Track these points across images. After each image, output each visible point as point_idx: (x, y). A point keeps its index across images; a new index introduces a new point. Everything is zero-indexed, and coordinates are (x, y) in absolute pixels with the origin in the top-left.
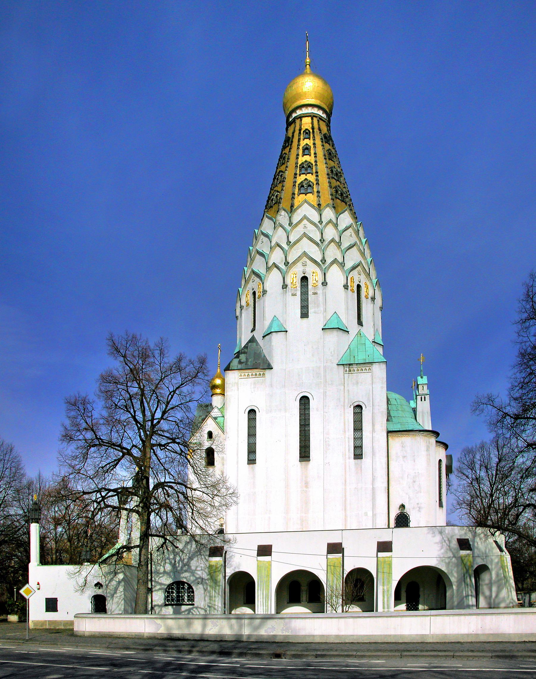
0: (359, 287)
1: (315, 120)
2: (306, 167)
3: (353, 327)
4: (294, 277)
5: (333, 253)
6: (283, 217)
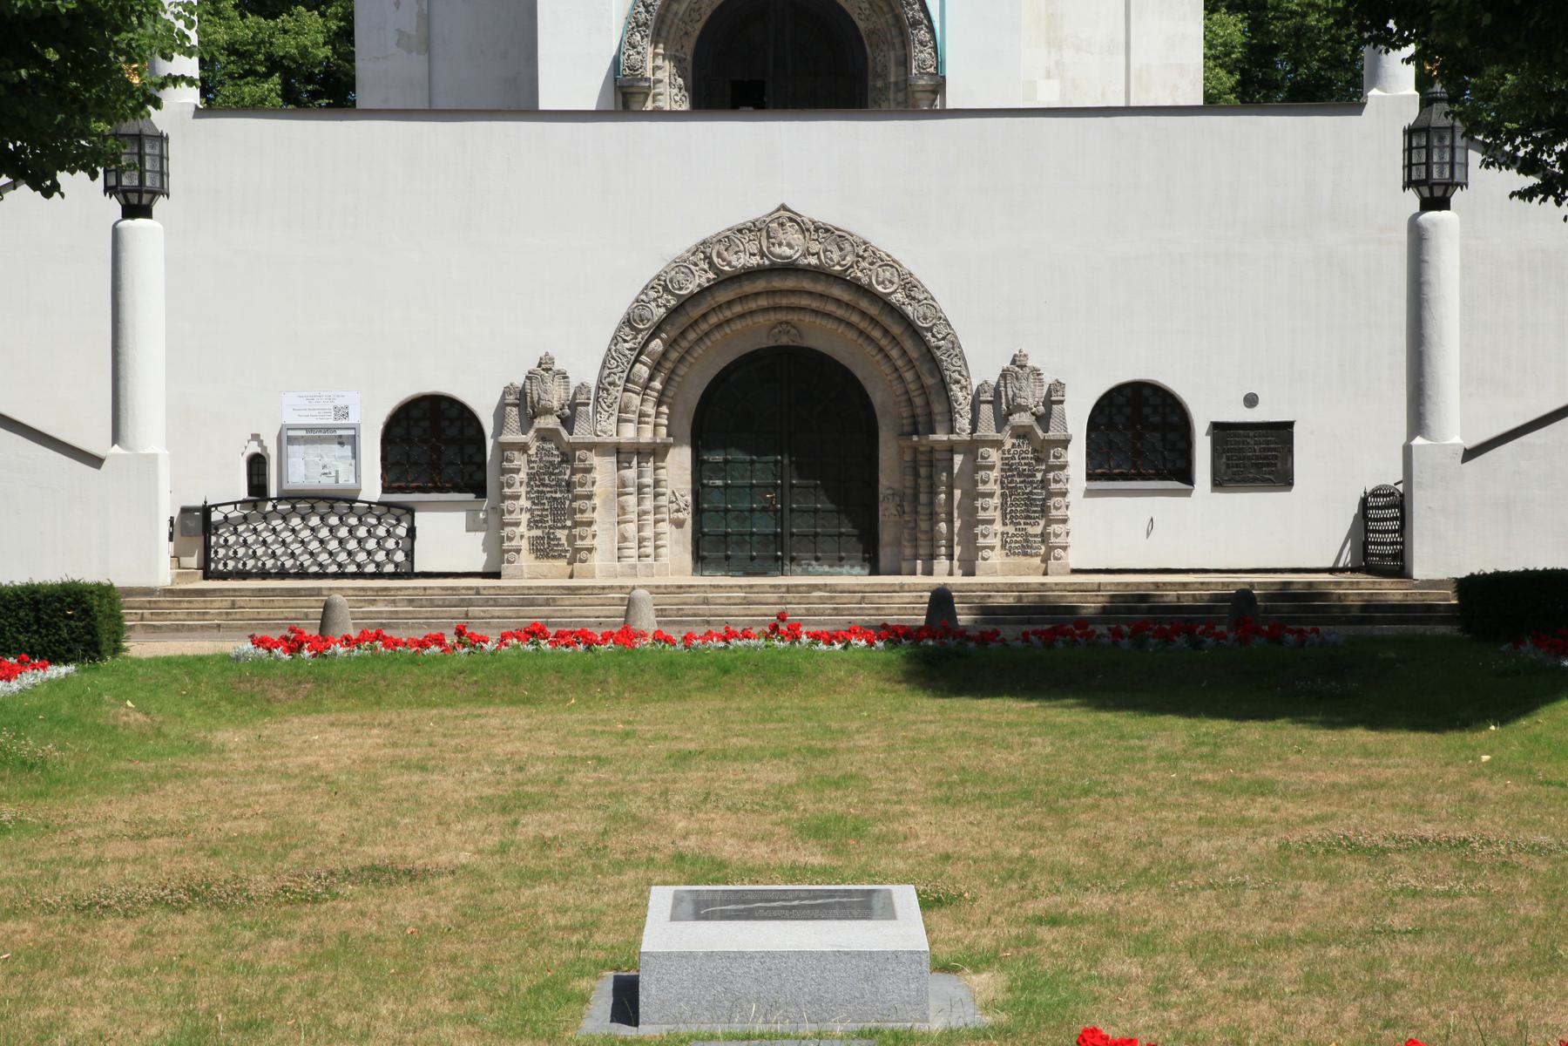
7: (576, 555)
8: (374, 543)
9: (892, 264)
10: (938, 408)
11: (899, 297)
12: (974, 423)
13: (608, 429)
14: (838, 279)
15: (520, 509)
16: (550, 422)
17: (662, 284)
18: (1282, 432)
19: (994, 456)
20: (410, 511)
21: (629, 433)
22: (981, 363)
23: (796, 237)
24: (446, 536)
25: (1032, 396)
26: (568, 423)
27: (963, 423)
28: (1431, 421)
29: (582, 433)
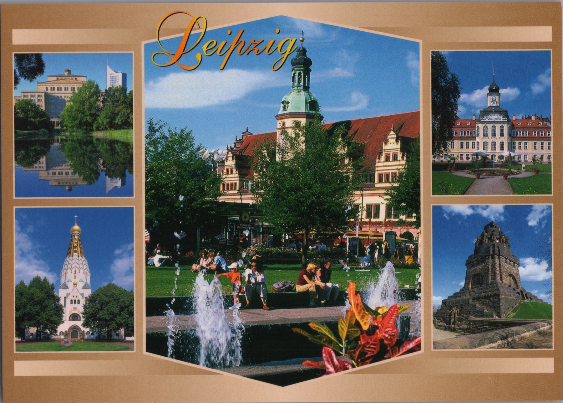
2: (76, 247)
3: (85, 281)
4: (73, 271)
5: (81, 266)
6: (71, 258)
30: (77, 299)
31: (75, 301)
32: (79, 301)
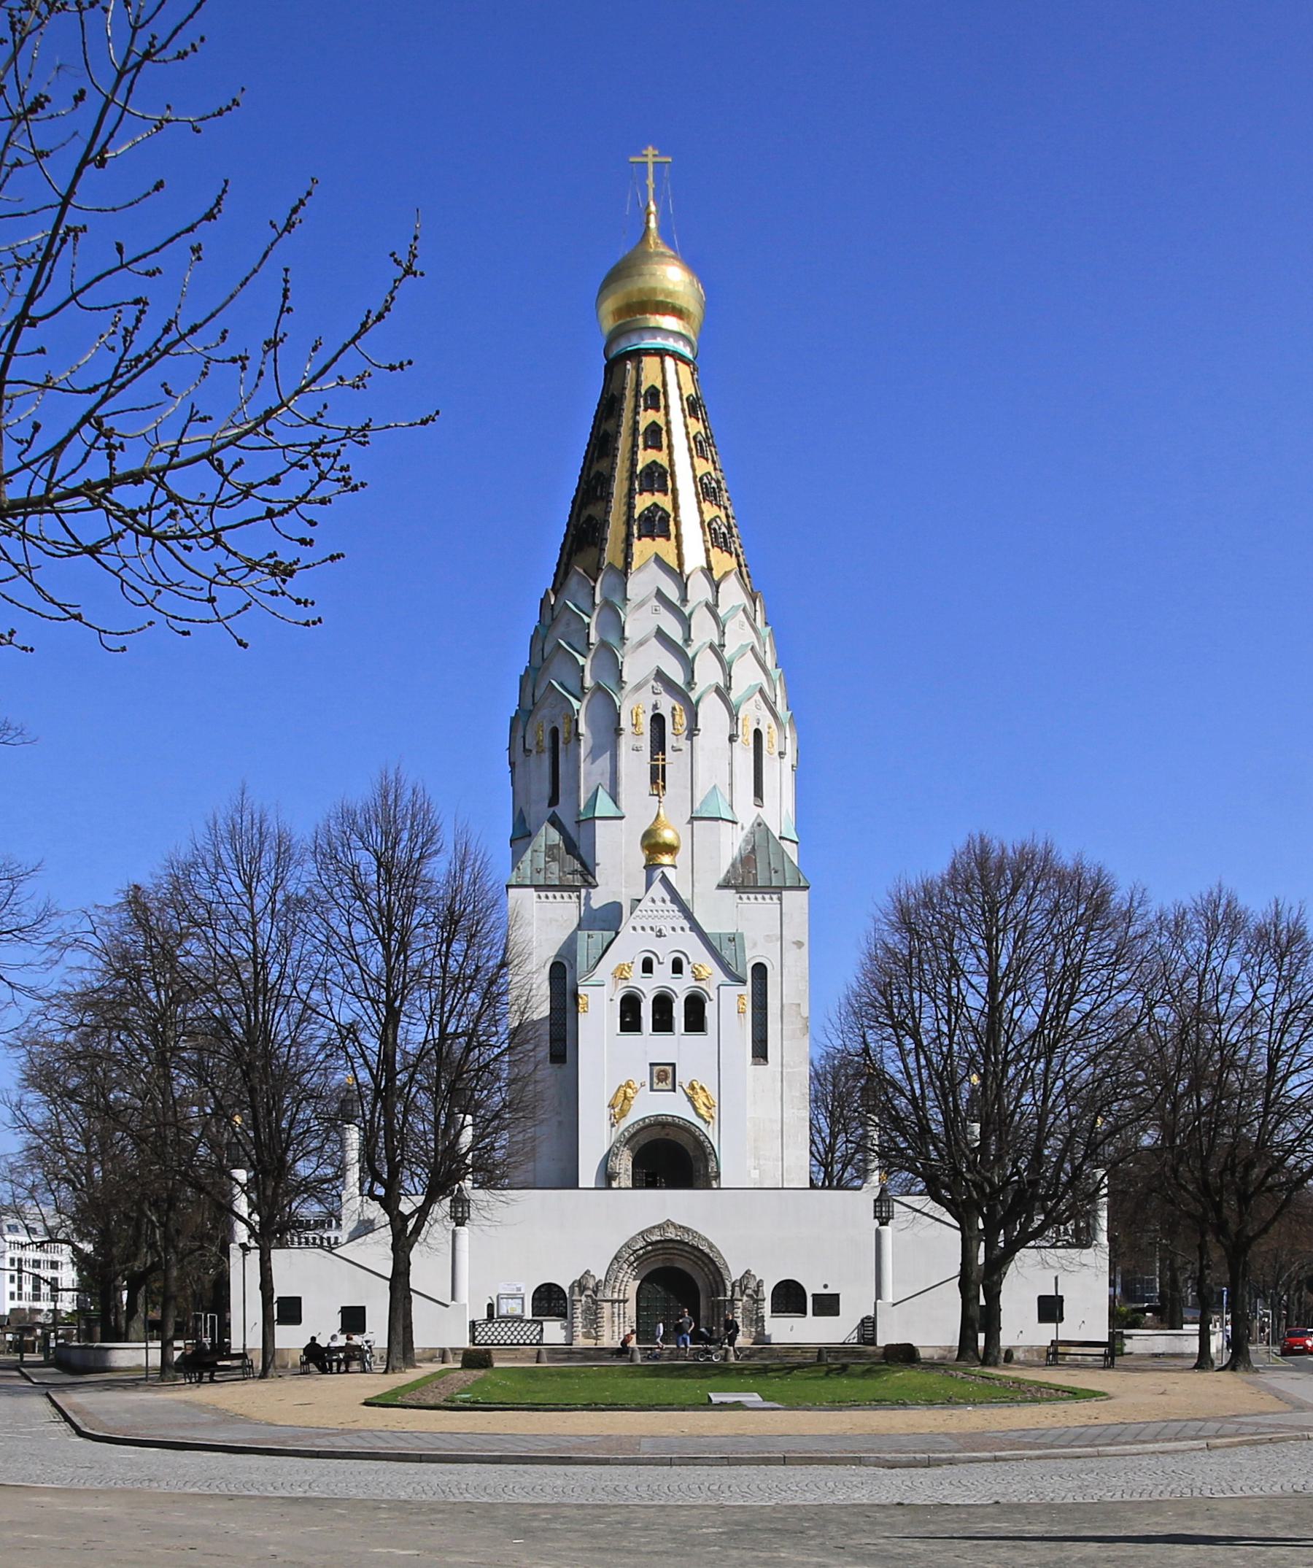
0: (758, 734)
1: (669, 362)
3: (746, 812)
7: (596, 1338)
8: (530, 1332)
9: (706, 1239)
10: (721, 1288)
11: (707, 1250)
12: (733, 1291)
13: (609, 1295)
14: (687, 1244)
15: (579, 1321)
16: (589, 1293)
17: (627, 1245)
18: (835, 1298)
19: (740, 1304)
20: (541, 1323)
21: (616, 1296)
22: (735, 1273)
23: (672, 1229)
24: (554, 1332)
25: (752, 1285)
26: (595, 1293)
27: (729, 1293)
28: (884, 1295)
29: (600, 1296)
30: (681, 988)
31: (663, 1003)
32: (695, 1006)
